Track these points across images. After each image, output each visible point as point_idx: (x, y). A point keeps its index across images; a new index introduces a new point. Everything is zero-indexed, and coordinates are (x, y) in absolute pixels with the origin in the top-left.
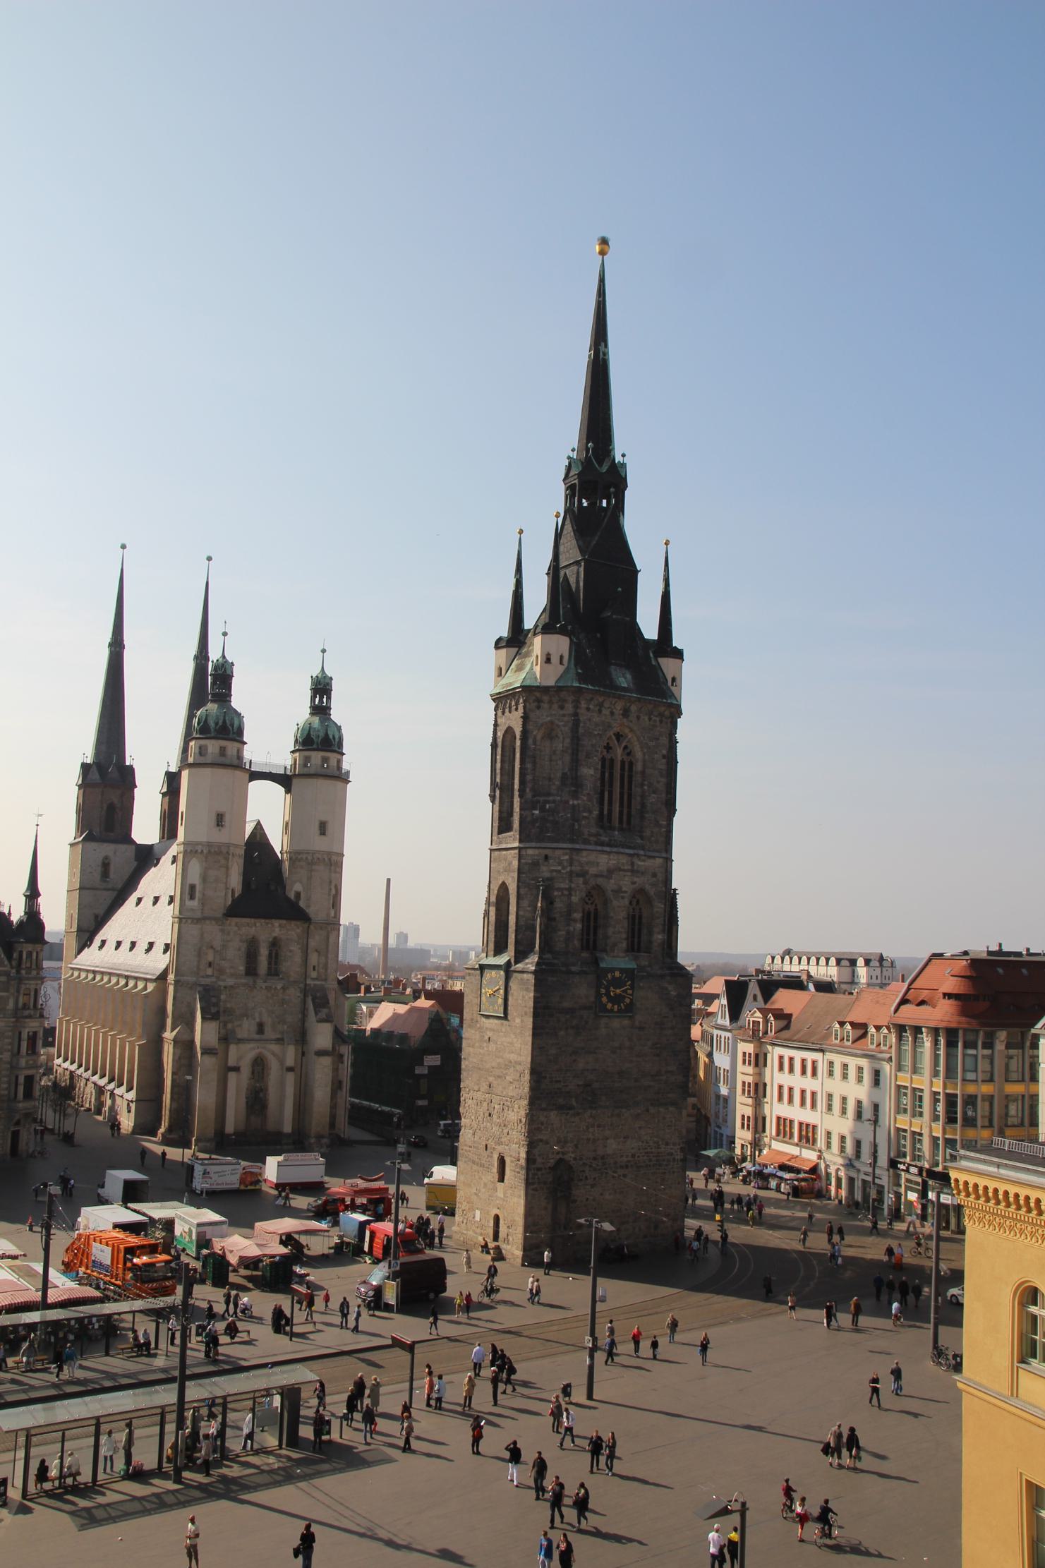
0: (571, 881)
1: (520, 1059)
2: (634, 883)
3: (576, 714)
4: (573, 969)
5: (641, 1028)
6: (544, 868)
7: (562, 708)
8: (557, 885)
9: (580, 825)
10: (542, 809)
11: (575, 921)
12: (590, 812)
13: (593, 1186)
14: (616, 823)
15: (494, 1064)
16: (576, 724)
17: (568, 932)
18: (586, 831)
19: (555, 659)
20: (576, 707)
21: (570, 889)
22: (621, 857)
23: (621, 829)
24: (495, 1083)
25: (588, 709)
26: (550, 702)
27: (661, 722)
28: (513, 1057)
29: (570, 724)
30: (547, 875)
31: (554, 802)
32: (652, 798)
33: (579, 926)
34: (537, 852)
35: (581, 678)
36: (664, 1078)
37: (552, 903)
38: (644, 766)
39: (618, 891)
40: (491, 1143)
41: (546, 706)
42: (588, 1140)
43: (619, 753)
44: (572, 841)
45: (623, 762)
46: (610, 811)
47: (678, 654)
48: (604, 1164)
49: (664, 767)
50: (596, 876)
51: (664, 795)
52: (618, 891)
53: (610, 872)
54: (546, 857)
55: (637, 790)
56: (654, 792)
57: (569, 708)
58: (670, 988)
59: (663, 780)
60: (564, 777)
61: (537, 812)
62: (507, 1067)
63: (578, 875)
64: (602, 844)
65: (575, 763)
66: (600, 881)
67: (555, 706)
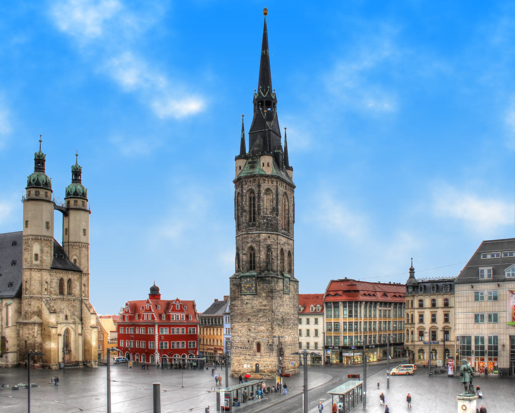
1: (266, 308)
3: (277, 186)
6: (269, 241)
7: (272, 183)
10: (267, 220)
16: (277, 189)
20: (277, 184)
24: (252, 318)
26: (268, 181)
30: (269, 243)
31: (271, 217)
34: (266, 235)
38: (289, 207)
39: (286, 251)
40: (251, 339)
41: (267, 182)
44: (277, 231)
47: (291, 169)
62: (259, 311)
65: (277, 203)
67: (270, 182)
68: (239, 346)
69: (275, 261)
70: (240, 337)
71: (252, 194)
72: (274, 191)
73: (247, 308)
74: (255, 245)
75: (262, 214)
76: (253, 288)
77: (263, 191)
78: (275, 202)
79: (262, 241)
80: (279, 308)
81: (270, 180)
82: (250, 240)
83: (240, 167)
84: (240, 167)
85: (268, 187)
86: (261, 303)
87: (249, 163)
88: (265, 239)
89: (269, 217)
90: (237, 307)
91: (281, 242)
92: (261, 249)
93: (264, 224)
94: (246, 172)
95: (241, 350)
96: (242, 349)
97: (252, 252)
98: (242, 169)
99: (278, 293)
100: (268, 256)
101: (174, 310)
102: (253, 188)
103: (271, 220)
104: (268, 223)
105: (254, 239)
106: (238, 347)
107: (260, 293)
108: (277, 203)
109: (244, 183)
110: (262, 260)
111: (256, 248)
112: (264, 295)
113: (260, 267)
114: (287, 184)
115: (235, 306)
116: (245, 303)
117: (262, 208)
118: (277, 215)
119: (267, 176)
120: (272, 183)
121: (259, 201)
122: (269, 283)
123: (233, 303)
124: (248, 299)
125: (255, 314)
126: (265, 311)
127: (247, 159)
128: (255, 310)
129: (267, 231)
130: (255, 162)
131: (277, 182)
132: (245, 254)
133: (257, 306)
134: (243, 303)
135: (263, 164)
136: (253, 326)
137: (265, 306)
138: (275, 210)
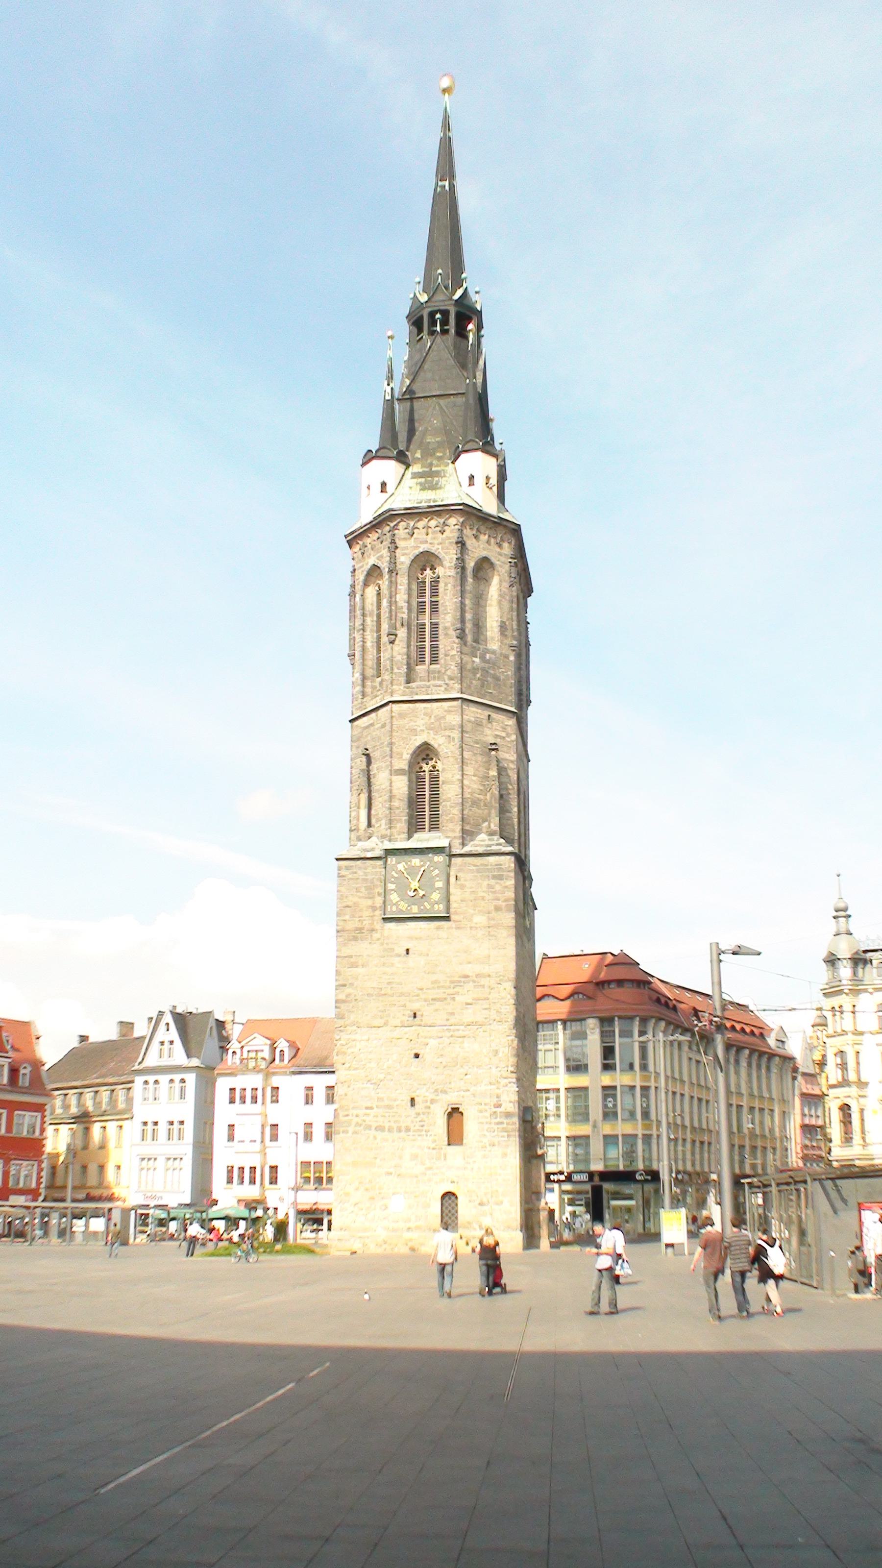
1: (486, 970)
6: (488, 731)
10: (483, 658)
28: (469, 970)
61: (477, 660)
62: (456, 983)
70: (377, 1085)
71: (428, 572)
76: (436, 896)
83: (384, 485)
84: (384, 485)
85: (484, 554)
87: (415, 476)
88: (478, 724)
90: (363, 966)
93: (475, 670)
95: (380, 1135)
96: (386, 1134)
97: (426, 768)
98: (390, 488)
103: (494, 664)
105: (439, 719)
106: (369, 1127)
109: (401, 532)
110: (467, 795)
112: (480, 919)
115: (354, 965)
123: (346, 951)
124: (411, 938)
126: (483, 981)
129: (483, 697)
130: (437, 474)
132: (400, 772)
136: (433, 1042)
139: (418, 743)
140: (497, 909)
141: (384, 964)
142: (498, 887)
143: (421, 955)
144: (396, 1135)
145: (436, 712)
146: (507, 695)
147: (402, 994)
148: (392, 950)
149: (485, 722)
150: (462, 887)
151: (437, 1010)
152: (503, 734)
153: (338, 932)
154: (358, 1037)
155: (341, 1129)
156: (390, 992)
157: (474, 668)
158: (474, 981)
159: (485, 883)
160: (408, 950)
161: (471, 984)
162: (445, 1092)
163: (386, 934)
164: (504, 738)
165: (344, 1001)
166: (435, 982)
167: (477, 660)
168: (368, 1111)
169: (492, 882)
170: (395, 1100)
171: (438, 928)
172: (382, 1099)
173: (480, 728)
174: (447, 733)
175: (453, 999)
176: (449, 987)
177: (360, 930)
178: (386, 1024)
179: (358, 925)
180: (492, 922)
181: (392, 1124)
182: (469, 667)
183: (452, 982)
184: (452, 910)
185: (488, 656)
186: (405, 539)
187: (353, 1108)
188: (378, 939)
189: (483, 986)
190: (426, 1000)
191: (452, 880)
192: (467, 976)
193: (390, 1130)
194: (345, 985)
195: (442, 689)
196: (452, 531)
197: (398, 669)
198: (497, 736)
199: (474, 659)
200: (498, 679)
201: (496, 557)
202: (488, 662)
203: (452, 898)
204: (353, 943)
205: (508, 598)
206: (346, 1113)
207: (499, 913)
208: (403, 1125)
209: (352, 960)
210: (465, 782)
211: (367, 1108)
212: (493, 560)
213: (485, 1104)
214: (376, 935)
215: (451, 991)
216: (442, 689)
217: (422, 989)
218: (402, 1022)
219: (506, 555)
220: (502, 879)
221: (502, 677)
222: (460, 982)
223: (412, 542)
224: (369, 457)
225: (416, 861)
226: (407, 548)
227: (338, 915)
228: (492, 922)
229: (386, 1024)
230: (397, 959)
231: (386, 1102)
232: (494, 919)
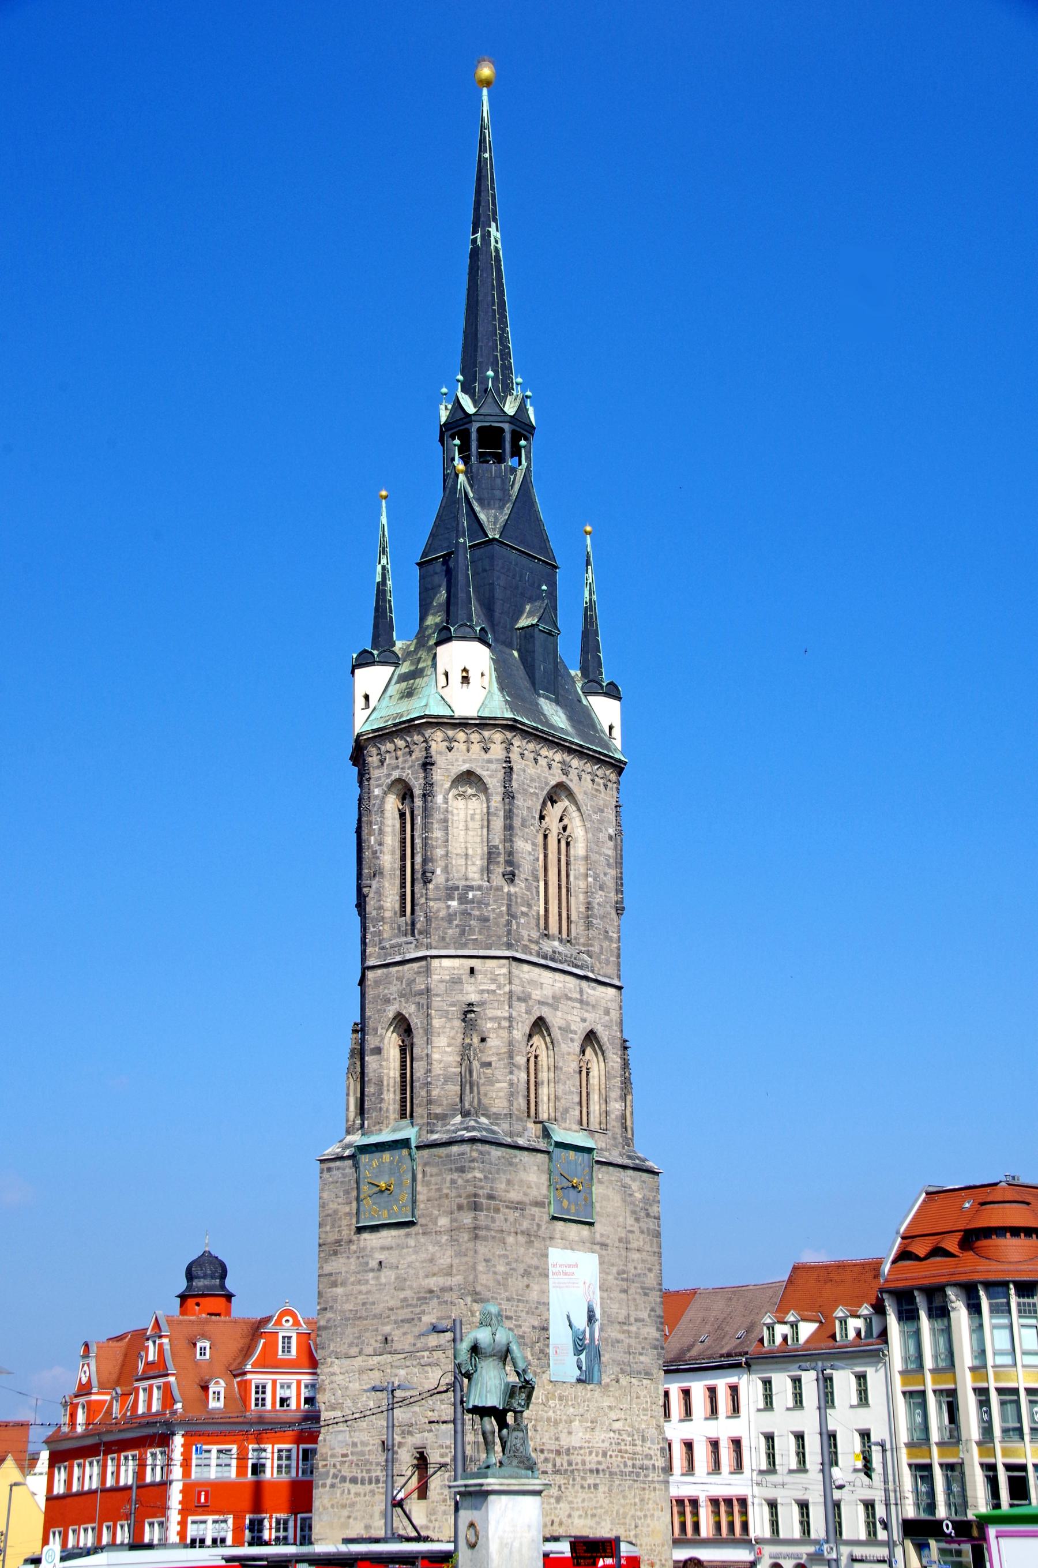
0: (510, 1007)
1: (449, 1282)
2: (584, 1020)
4: (521, 1142)
5: (604, 1245)
7: (486, 750)
8: (490, 1013)
9: (518, 924)
10: (463, 899)
11: (519, 1068)
12: (529, 906)
13: (558, 1500)
14: (553, 928)
15: (392, 1303)
17: (511, 1084)
18: (524, 933)
19: (474, 676)
20: (508, 750)
21: (510, 1019)
22: (568, 978)
23: (561, 940)
24: (397, 1335)
25: (522, 755)
27: (606, 786)
28: (433, 1283)
29: (501, 774)
30: (473, 998)
31: (480, 888)
32: (599, 897)
33: (523, 1076)
34: (457, 962)
35: (512, 706)
36: (633, 1328)
37: (483, 1040)
39: (566, 1030)
41: (463, 747)
42: (549, 1420)
43: (555, 828)
44: (509, 946)
45: (559, 841)
46: (546, 910)
48: (570, 1464)
49: (610, 852)
50: (541, 1003)
51: (612, 894)
52: (566, 1030)
53: (554, 1002)
54: (472, 971)
55: (578, 885)
56: (601, 888)
57: (497, 751)
58: (635, 1186)
59: (612, 872)
60: (491, 856)
61: (454, 904)
62: (423, 1300)
63: (519, 999)
64: (545, 957)
66: (546, 1012)
67: (476, 748)
68: (346, 1472)
69: (499, 1074)
72: (494, 782)
73: (381, 1287)
74: (412, 1008)
75: (439, 877)
77: (442, 776)
78: (498, 823)
79: (442, 987)
80: (516, 1284)
81: (475, 737)
82: (394, 989)
84: (367, 697)
85: (465, 767)
86: (431, 1260)
89: (471, 888)
90: (343, 1284)
91: (536, 994)
92: (436, 1023)
93: (450, 918)
94: (383, 713)
95: (354, 1488)
98: (373, 702)
99: (513, 1215)
100: (465, 1052)
101: (270, 1362)
102: (408, 775)
103: (480, 903)
104: (465, 913)
106: (344, 1479)
107: (430, 1215)
108: (509, 828)
110: (437, 1069)
111: (416, 1022)
112: (444, 1221)
113: (430, 1102)
114: (570, 751)
115: (334, 1284)
116: (373, 1264)
117: (439, 852)
118: (511, 877)
119: (463, 724)
120: (486, 750)
121: (426, 827)
122: (462, 1170)
123: (328, 1268)
124: (383, 1248)
125: (404, 1314)
126: (447, 1297)
127: (397, 665)
128: (408, 1293)
129: (464, 946)
131: (508, 746)
133: (417, 1275)
134: (365, 1268)
135: (446, 674)
137: (449, 1272)
138: (502, 860)
139: (391, 1015)
140: (460, 1207)
141: (359, 1282)
142: (460, 1182)
143: (391, 1268)
144: (368, 1488)
145: (408, 975)
146: (499, 937)
147: (375, 1316)
148: (367, 1263)
149: (466, 977)
150: (427, 1184)
151: (405, 1334)
152: (493, 987)
153: (320, 1245)
154: (336, 1369)
155: (320, 1482)
156: (364, 1314)
157: (450, 915)
158: (438, 1297)
159: (449, 1178)
160: (380, 1262)
161: (435, 1300)
162: (410, 1433)
163: (362, 1244)
164: (494, 991)
165: (325, 1328)
166: (405, 1299)
167: (454, 904)
168: (344, 1459)
169: (455, 1176)
170: (367, 1444)
171: (408, 1235)
172: (354, 1445)
173: (456, 987)
174: (417, 999)
175: (420, 1319)
176: (416, 1306)
177: (338, 1242)
178: (360, 1353)
179: (336, 1237)
180: (455, 1224)
181: (364, 1474)
182: (442, 914)
183: (419, 1299)
184: (417, 1213)
185: (470, 895)
186: (378, 767)
187: (333, 1456)
188: (355, 1252)
189: (446, 1302)
190: (395, 1323)
191: (419, 1176)
192: (431, 1291)
193: (363, 1483)
194: (326, 1309)
195: (413, 946)
196: (421, 751)
197: (374, 927)
198: (482, 992)
199: (449, 903)
200: (486, 920)
201: (482, 768)
202: (472, 901)
203: (420, 1198)
204: (333, 1258)
205: (501, 813)
206: (324, 1463)
207: (461, 1212)
208: (374, 1475)
209: (333, 1278)
210: (436, 1056)
211: (343, 1456)
212: (479, 771)
213: (447, 1447)
214: (353, 1247)
215: (418, 1310)
216: (413, 946)
217: (392, 1309)
218: (375, 1350)
219: (497, 760)
220: (463, 1171)
221: (492, 916)
222: (426, 1298)
223: (384, 770)
224: (364, 660)
225: (387, 1156)
226: (379, 778)
227: (320, 1225)
228: (455, 1224)
229: (360, 1353)
230: (371, 1275)
231: (359, 1448)
232: (456, 1220)
